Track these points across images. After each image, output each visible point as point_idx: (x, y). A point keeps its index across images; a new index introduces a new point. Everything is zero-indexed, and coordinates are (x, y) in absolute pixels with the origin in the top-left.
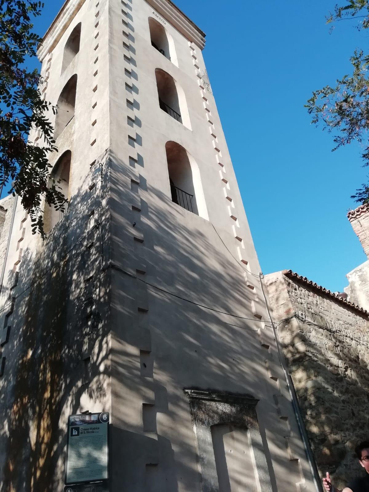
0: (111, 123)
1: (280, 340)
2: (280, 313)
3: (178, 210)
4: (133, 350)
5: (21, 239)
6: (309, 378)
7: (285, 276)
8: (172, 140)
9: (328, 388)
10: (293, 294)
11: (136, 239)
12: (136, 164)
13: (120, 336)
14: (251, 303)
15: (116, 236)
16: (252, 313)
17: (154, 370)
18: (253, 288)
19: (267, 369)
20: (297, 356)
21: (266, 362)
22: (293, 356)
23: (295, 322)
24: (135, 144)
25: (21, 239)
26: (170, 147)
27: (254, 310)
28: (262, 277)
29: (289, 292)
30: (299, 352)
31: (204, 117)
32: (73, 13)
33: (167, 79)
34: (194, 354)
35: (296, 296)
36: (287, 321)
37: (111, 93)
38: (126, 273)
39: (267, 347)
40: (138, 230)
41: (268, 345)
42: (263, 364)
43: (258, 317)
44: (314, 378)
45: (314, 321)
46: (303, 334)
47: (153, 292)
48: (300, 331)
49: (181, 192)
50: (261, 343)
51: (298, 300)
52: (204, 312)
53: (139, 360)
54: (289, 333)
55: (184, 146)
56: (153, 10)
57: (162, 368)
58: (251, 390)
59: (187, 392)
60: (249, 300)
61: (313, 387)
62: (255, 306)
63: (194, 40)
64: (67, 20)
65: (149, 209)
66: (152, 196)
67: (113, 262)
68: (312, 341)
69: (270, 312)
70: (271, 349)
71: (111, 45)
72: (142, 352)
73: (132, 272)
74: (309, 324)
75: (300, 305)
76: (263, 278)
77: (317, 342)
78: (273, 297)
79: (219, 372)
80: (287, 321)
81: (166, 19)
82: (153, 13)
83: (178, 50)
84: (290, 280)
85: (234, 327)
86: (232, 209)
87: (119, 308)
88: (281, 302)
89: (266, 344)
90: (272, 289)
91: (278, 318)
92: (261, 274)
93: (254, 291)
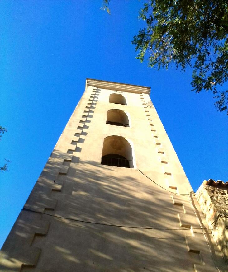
3: (105, 167)
10: (219, 198)
26: (114, 140)
28: (193, 195)
29: (212, 197)
33: (120, 112)
40: (60, 184)
65: (76, 171)
66: (87, 166)
73: (42, 210)
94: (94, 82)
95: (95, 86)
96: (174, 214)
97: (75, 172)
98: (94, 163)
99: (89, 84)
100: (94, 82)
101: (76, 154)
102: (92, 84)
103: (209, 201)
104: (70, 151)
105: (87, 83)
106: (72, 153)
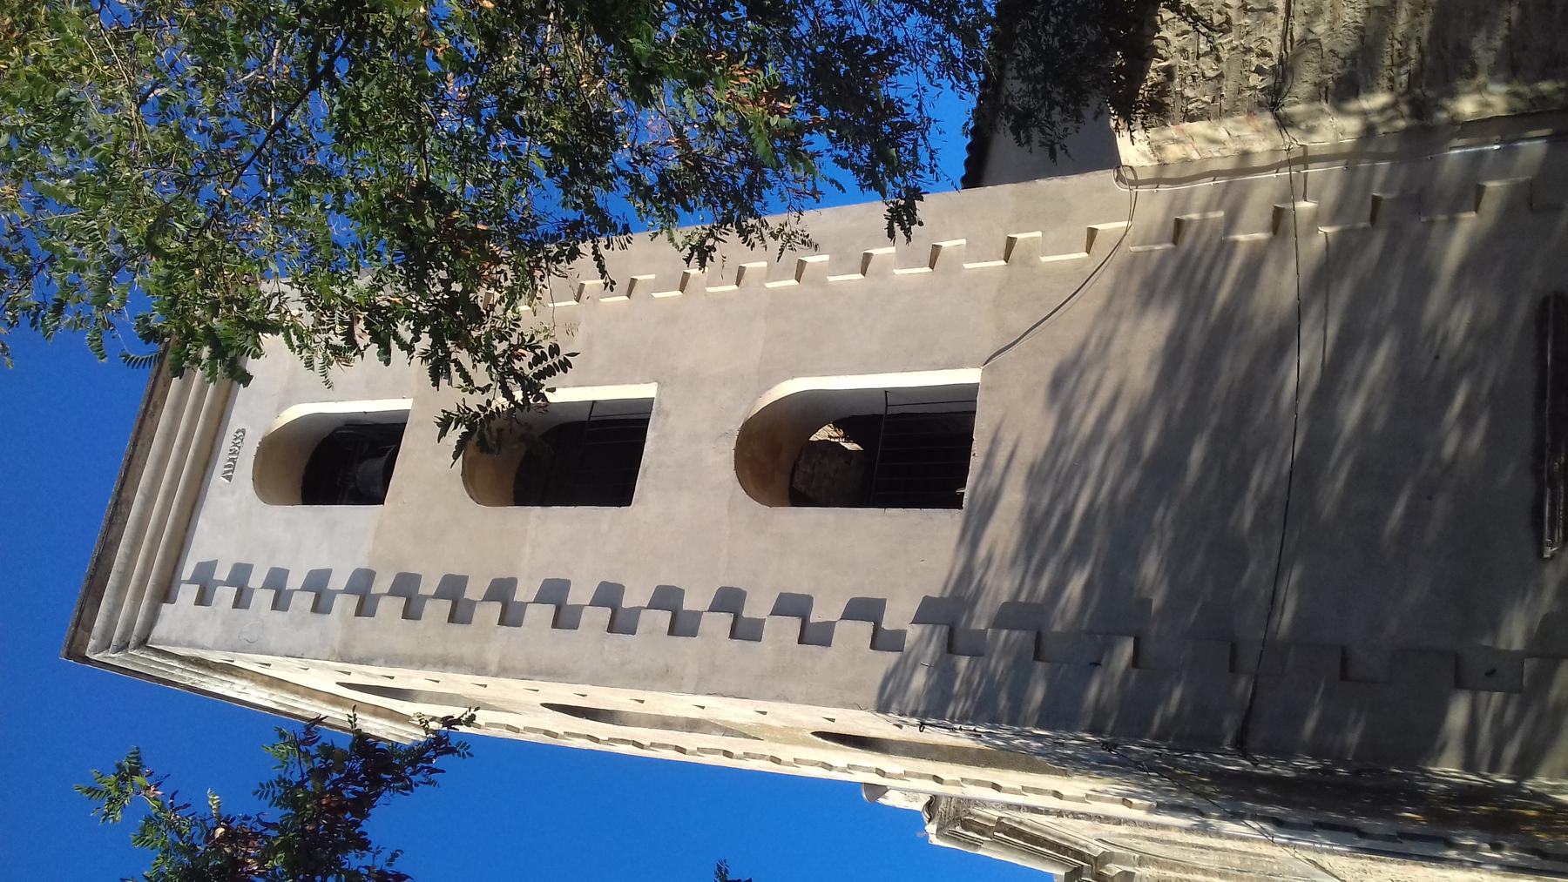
0: (786, 699)
1: (1348, 140)
6: (1481, 89)
9: (1509, 21)
10: (1189, 93)
11: (1136, 660)
12: (886, 625)
13: (1428, 742)
14: (1235, 242)
15: (1149, 722)
16: (1270, 241)
17: (1502, 646)
18: (1179, 224)
19: (1452, 222)
20: (1405, 108)
24: (814, 618)
28: (1130, 176)
29: (1192, 119)
30: (1394, 105)
32: (296, 693)
34: (1442, 506)
35: (1194, 79)
38: (1252, 701)
40: (1108, 646)
41: (1370, 201)
42: (1436, 231)
43: (1279, 220)
44: (1481, 78)
47: (1287, 618)
49: (903, 453)
52: (1306, 444)
53: (1483, 695)
55: (735, 428)
56: (217, 479)
58: (1523, 308)
59: (1553, 555)
60: (1227, 248)
61: (1507, 82)
64: (315, 702)
65: (1022, 598)
67: (1229, 740)
68: (1353, 47)
69: (1257, 162)
71: (493, 668)
72: (1460, 684)
73: (1243, 685)
79: (1482, 423)
80: (1284, 123)
81: (217, 430)
82: (229, 478)
85: (1332, 330)
88: (1222, 134)
89: (1367, 213)
90: (1173, 152)
92: (1119, 178)
94: (118, 608)
95: (166, 593)
97: (1025, 604)
98: (972, 536)
99: (133, 640)
100: (117, 606)
102: (140, 619)
103: (1199, 127)
104: (880, 640)
105: (123, 647)
106: (902, 633)
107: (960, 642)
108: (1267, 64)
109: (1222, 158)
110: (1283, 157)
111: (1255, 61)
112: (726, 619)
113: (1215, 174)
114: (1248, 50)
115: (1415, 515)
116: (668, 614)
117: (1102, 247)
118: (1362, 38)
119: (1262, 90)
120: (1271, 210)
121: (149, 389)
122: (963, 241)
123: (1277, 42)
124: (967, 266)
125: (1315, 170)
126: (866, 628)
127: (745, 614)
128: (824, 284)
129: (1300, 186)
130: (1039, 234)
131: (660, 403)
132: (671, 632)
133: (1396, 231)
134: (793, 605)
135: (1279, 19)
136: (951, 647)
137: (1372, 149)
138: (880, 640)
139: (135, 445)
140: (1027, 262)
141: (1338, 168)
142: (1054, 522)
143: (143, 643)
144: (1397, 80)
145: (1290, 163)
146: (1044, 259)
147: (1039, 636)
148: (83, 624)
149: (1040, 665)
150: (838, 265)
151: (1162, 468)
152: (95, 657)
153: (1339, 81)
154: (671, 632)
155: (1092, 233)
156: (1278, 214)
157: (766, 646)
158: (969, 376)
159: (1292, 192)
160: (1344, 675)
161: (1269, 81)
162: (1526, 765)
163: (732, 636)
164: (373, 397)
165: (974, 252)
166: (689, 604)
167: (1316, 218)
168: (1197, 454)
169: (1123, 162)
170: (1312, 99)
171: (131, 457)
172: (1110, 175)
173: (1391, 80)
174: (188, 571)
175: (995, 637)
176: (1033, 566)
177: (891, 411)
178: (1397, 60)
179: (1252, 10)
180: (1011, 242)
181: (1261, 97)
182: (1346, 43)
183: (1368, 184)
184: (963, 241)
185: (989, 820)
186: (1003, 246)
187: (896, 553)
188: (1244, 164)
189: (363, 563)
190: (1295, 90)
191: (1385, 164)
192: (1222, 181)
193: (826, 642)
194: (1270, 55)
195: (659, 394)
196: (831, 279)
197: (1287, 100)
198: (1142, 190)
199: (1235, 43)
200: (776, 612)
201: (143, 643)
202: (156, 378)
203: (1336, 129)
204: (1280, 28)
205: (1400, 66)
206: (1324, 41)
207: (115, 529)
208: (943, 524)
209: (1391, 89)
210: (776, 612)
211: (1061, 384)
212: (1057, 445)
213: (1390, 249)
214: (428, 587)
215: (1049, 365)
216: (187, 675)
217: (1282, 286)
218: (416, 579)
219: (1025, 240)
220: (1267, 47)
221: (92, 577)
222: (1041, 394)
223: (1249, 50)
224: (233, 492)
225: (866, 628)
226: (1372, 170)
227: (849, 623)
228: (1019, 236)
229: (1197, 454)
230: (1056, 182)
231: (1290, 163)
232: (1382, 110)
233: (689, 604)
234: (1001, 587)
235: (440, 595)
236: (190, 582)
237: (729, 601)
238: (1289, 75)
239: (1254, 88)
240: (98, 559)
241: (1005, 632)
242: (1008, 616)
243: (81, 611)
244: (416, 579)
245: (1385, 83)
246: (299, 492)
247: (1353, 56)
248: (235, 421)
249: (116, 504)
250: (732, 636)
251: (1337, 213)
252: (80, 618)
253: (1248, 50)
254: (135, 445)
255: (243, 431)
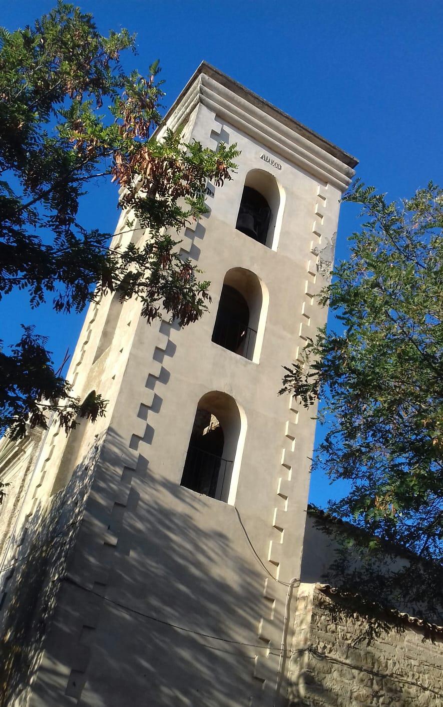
0: (120, 393)
1: (289, 675)
2: (297, 640)
4: (64, 669)
5: (39, 486)
7: (318, 592)
8: (215, 390)
10: (323, 617)
11: (108, 544)
13: (54, 654)
14: (260, 622)
16: (257, 635)
18: (272, 601)
21: (250, 700)
22: (294, 699)
23: (307, 657)
24: (150, 412)
25: (39, 486)
27: (260, 631)
28: (296, 585)
29: (313, 616)
31: (293, 331)
35: (328, 621)
36: (301, 652)
37: (134, 346)
39: (263, 681)
40: (115, 534)
43: (265, 641)
45: (347, 658)
46: (313, 674)
48: (307, 670)
50: (253, 674)
51: (329, 626)
54: (298, 668)
55: (233, 395)
56: (263, 152)
57: (95, 690)
60: (259, 616)
62: (263, 627)
63: (329, 178)
65: (140, 503)
68: (325, 685)
69: (289, 638)
70: (267, 686)
72: (73, 671)
74: (332, 661)
75: (329, 634)
76: (299, 586)
77: (337, 688)
78: (299, 616)
80: (301, 652)
82: (262, 158)
83: (288, 214)
84: (328, 598)
86: (284, 484)
87: (61, 625)
88: (304, 626)
89: (259, 676)
90: (301, 605)
91: (296, 646)
93: (274, 605)
94: (219, 92)
95: (220, 117)
96: (255, 618)
97: (137, 502)
99: (203, 97)
100: (220, 93)
101: (144, 449)
103: (309, 618)
104: (135, 439)
105: (202, 91)
107: (128, 473)
108: (327, 651)
109: (294, 623)
110: (288, 648)
111: (329, 647)
112: (157, 374)
113: (288, 619)
114: (334, 645)
115: (140, 668)
116: (164, 349)
117: (270, 567)
118: (327, 690)
119: (317, 647)
120: (269, 638)
121: (309, 130)
122: (286, 510)
123: (334, 657)
124: (276, 509)
125: (280, 659)
126: (141, 434)
127: (157, 382)
128: (283, 447)
129: (276, 652)
130: (282, 542)
131: (250, 363)
132: (157, 348)
133: (249, 686)
134: (157, 403)
135: (342, 659)
136: (127, 469)
137: (283, 683)
138: (135, 439)
139: (287, 117)
140: (271, 535)
141: (279, 668)
142: (167, 522)
143: (201, 101)
144: (308, 700)
145: (285, 650)
146: (271, 542)
147: (124, 506)
148: (215, 75)
149: (113, 504)
150: (289, 455)
151: (181, 573)
152: (200, 77)
153: (313, 678)
154: (157, 348)
155: (277, 564)
156: (266, 641)
157: (142, 388)
158: (232, 500)
159: (274, 647)
160: (85, 627)
161: (320, 650)
162: (38, 688)
163: (150, 375)
164: (281, 233)
165: (281, 513)
166: (166, 358)
167: (262, 655)
168: (183, 588)
169: (302, 584)
170: (309, 665)
171: (282, 114)
172: (298, 577)
173: (309, 698)
174: (227, 129)
175: (127, 488)
176: (152, 511)
177: (222, 462)
178: (316, 702)
179: (349, 649)
180: (281, 530)
181: (314, 646)
182: (328, 683)
183: (270, 679)
184: (286, 510)
185: (26, 447)
186: (281, 527)
187: (168, 455)
188: (289, 632)
189: (213, 213)
190: (314, 659)
191: (276, 687)
192: (285, 621)
193: (139, 416)
194: (329, 653)
195: (254, 364)
196: (284, 450)
197: (311, 655)
198: (289, 588)
199: (338, 640)
200: (156, 396)
201: (201, 101)
202: (313, 134)
203: (293, 671)
204: (339, 659)
205: (313, 702)
206: (330, 675)
207: (253, 99)
208: (176, 476)
209: (305, 697)
210: (156, 396)
211: (220, 536)
212: (198, 530)
213: (243, 682)
214: (197, 241)
215: (230, 535)
216: (181, 112)
217: (240, 636)
218: (202, 237)
219: (280, 536)
220: (333, 652)
221: (234, 84)
222: (219, 529)
223: (333, 646)
224: (256, 158)
225: (141, 434)
226: (275, 682)
227: (145, 427)
228: (282, 534)
229: (183, 588)
230: (301, 554)
231: (285, 650)
232: (298, 691)
233: (166, 358)
234: (147, 494)
235: (193, 246)
236: (222, 129)
237: (164, 376)
238: (320, 659)
239: (319, 644)
240: (242, 89)
241: (128, 492)
242: (134, 494)
243: (221, 75)
244: (202, 237)
245: (308, 695)
246: (250, 186)
247: (321, 685)
248: (285, 166)
249: (263, 102)
250: (150, 375)
251: (262, 665)
252: (218, 74)
253: (334, 645)
254: (287, 117)
255: (280, 169)
